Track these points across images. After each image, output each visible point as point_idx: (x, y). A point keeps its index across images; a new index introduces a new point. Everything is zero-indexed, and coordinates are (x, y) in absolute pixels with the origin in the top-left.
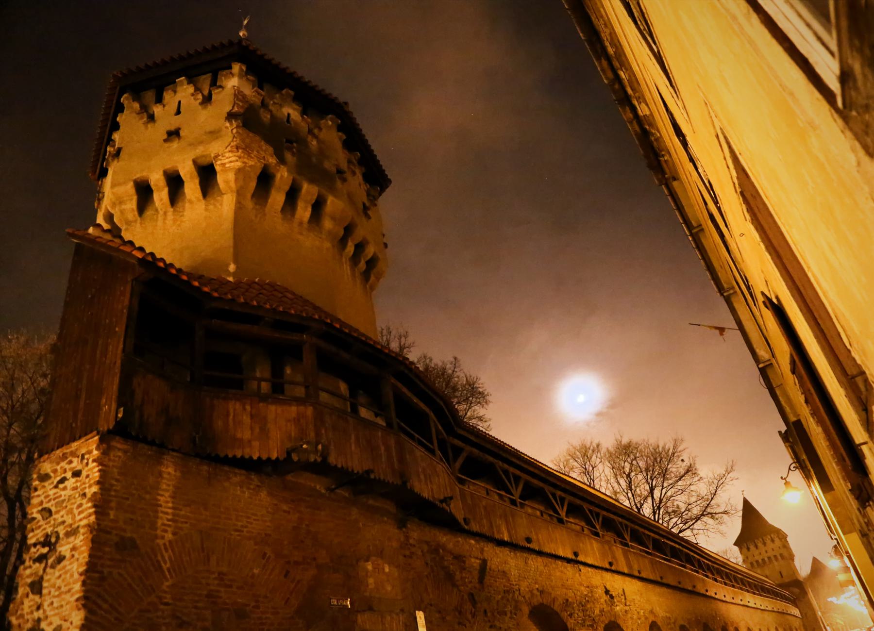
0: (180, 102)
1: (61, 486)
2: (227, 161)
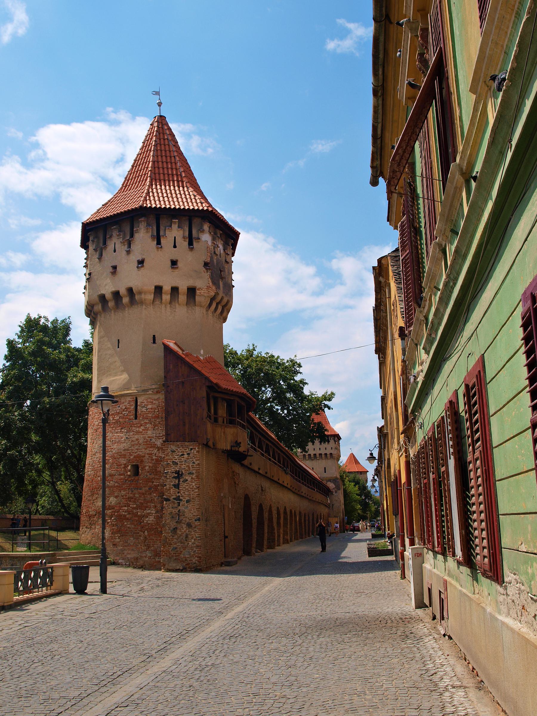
0: (175, 237)
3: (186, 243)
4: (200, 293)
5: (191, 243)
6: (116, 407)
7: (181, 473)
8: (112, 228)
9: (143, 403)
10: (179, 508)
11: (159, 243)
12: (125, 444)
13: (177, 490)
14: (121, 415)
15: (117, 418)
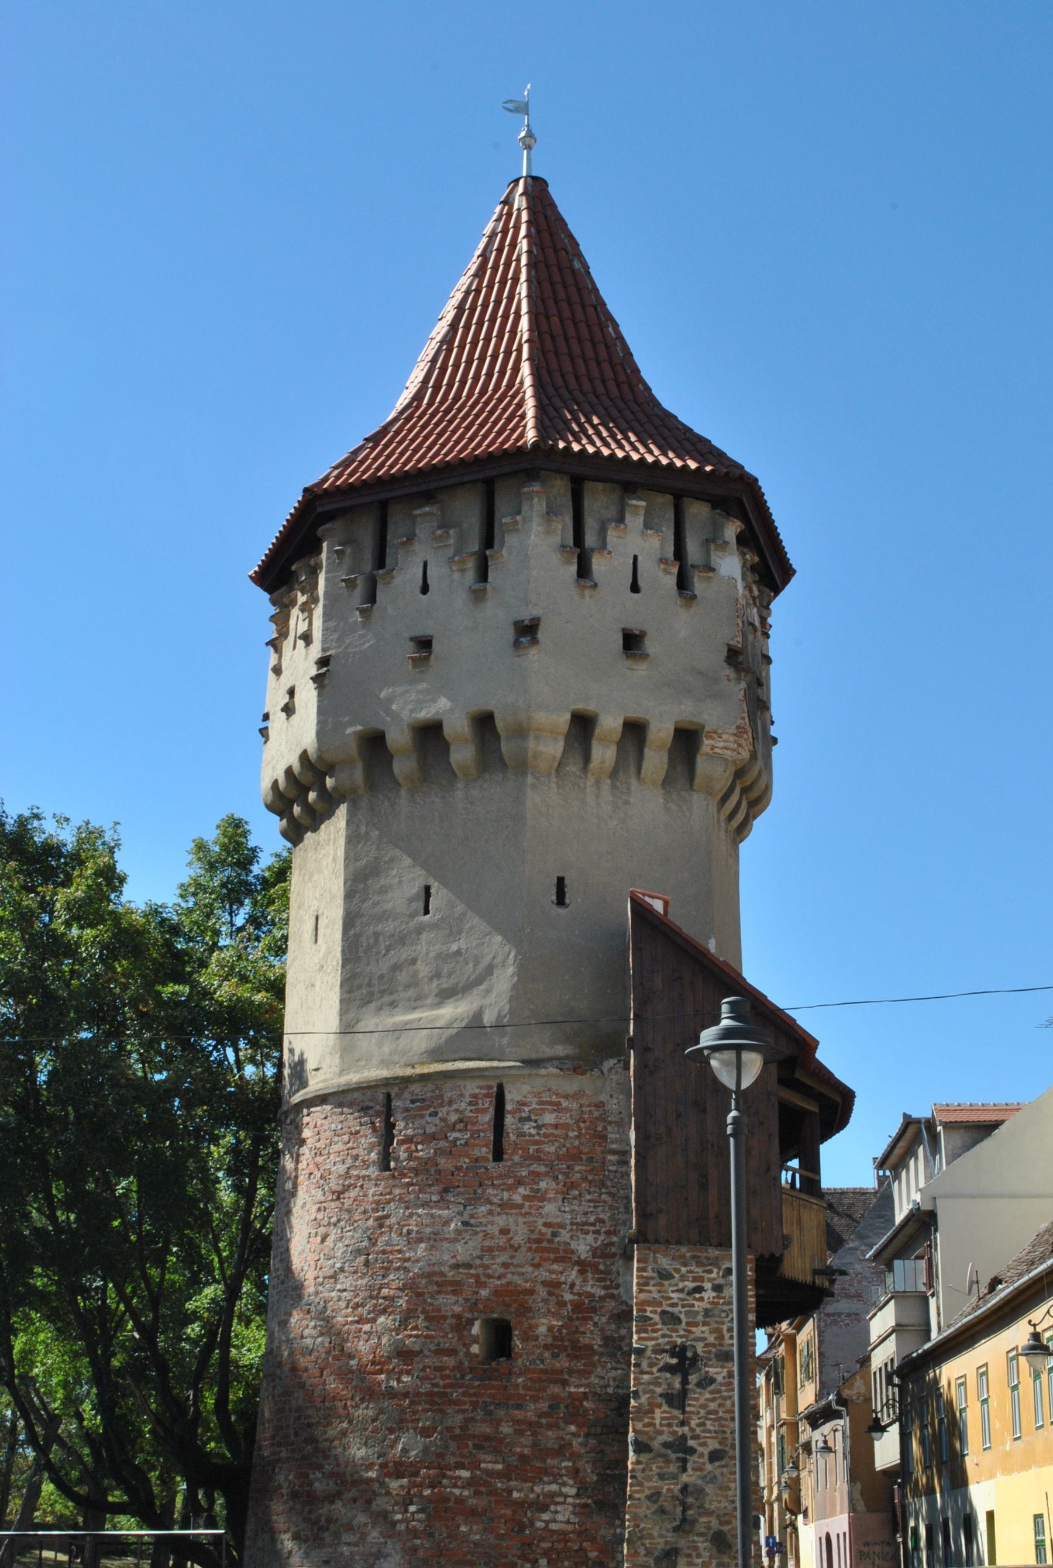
0: (635, 558)
1: (697, 1296)
2: (721, 744)
3: (671, 581)
4: (713, 748)
5: (683, 583)
6: (422, 1116)
7: (689, 1354)
8: (418, 512)
9: (524, 1104)
10: (684, 1478)
11: (584, 571)
12: (459, 1247)
13: (676, 1413)
14: (443, 1144)
15: (423, 1152)
